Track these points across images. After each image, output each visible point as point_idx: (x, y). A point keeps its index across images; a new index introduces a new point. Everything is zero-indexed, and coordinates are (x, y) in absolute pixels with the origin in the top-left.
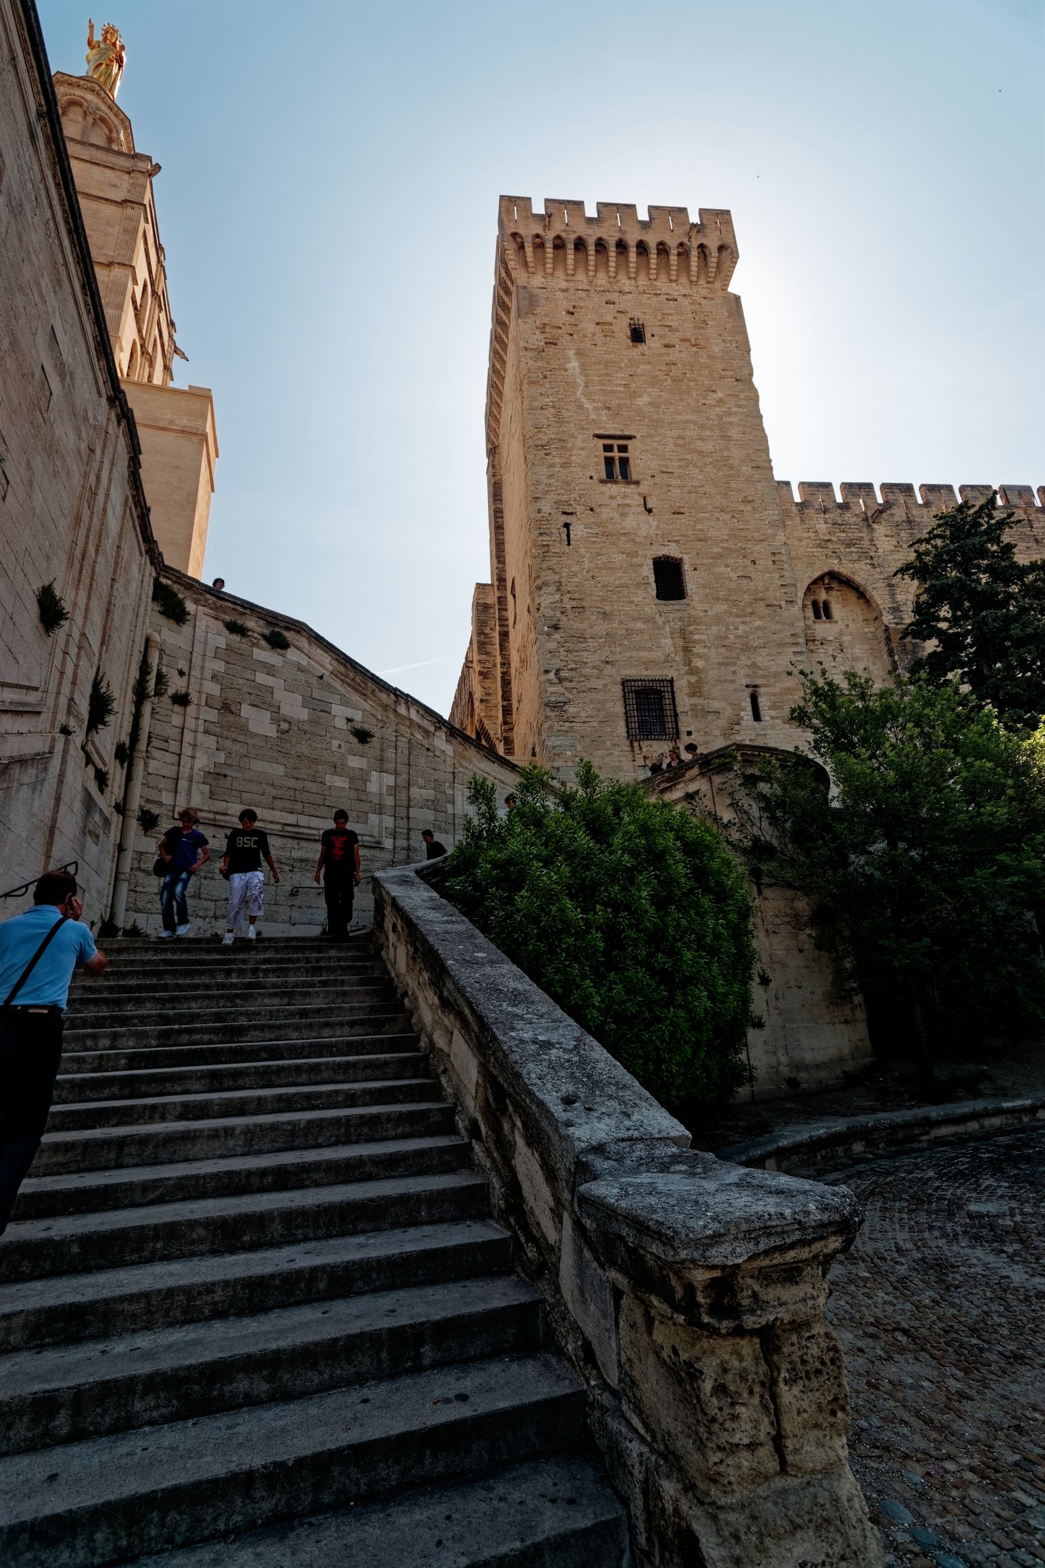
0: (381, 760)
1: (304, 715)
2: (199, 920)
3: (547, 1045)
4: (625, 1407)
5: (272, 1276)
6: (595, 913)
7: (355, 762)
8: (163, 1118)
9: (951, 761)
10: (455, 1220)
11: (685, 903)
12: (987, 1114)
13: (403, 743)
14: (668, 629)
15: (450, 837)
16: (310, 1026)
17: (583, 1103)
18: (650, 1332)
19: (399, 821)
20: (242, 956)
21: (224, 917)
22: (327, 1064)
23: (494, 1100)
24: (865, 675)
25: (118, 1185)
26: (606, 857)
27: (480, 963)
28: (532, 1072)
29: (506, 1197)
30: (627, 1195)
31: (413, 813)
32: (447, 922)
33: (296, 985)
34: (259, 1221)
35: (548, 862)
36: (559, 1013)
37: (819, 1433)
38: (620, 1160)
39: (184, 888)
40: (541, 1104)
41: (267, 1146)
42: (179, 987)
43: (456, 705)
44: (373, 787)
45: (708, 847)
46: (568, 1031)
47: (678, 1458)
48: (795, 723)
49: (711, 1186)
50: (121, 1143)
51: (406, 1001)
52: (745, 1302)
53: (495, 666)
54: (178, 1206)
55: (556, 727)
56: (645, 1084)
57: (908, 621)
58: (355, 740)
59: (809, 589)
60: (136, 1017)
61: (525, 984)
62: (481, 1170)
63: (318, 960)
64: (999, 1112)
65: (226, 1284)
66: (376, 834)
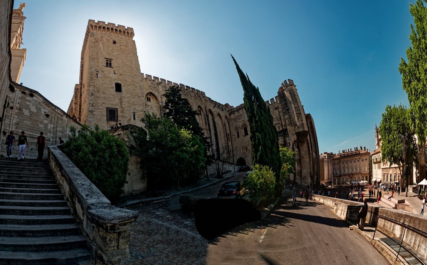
0: (51, 121)
1: (35, 111)
2: (13, 154)
3: (84, 185)
4: (93, 242)
5: (31, 220)
6: (96, 158)
7: (45, 122)
8: (9, 192)
9: (169, 134)
10: (63, 215)
11: (115, 157)
12: (163, 199)
13: (56, 118)
14: (117, 98)
15: (65, 139)
16: (35, 177)
17: (90, 196)
18: (99, 233)
19: (54, 135)
20: (21, 162)
21: (18, 154)
22: (38, 185)
23: (72, 194)
24: (156, 114)
25: (4, 202)
26: (99, 146)
27: (70, 167)
28: (80, 190)
29: (73, 211)
30: (97, 212)
31: (57, 133)
32: (63, 158)
33: (32, 169)
34: (28, 211)
35: (86, 146)
36: (86, 178)
37: (124, 245)
38: (96, 206)
39: (11, 147)
40: (81, 196)
41: (28, 199)
42: (10, 167)
43: (69, 110)
44: (49, 127)
45: (122, 146)
46: (88, 182)
47: (101, 248)
48: (142, 122)
49: (113, 211)
50: (3, 195)
51: (54, 174)
52: (116, 229)
53: (78, 102)
54: (14, 207)
55: (91, 116)
56: (103, 193)
57: (164, 105)
58: (46, 117)
59: (146, 95)
60: (3, 172)
61: (80, 172)
62: (69, 207)
63: (36, 164)
64: (164, 198)
65: (23, 220)
66: (49, 138)
